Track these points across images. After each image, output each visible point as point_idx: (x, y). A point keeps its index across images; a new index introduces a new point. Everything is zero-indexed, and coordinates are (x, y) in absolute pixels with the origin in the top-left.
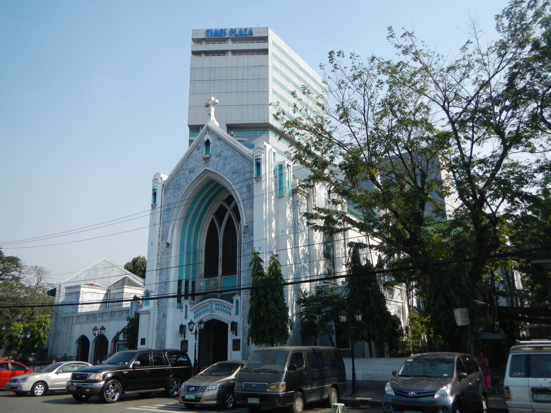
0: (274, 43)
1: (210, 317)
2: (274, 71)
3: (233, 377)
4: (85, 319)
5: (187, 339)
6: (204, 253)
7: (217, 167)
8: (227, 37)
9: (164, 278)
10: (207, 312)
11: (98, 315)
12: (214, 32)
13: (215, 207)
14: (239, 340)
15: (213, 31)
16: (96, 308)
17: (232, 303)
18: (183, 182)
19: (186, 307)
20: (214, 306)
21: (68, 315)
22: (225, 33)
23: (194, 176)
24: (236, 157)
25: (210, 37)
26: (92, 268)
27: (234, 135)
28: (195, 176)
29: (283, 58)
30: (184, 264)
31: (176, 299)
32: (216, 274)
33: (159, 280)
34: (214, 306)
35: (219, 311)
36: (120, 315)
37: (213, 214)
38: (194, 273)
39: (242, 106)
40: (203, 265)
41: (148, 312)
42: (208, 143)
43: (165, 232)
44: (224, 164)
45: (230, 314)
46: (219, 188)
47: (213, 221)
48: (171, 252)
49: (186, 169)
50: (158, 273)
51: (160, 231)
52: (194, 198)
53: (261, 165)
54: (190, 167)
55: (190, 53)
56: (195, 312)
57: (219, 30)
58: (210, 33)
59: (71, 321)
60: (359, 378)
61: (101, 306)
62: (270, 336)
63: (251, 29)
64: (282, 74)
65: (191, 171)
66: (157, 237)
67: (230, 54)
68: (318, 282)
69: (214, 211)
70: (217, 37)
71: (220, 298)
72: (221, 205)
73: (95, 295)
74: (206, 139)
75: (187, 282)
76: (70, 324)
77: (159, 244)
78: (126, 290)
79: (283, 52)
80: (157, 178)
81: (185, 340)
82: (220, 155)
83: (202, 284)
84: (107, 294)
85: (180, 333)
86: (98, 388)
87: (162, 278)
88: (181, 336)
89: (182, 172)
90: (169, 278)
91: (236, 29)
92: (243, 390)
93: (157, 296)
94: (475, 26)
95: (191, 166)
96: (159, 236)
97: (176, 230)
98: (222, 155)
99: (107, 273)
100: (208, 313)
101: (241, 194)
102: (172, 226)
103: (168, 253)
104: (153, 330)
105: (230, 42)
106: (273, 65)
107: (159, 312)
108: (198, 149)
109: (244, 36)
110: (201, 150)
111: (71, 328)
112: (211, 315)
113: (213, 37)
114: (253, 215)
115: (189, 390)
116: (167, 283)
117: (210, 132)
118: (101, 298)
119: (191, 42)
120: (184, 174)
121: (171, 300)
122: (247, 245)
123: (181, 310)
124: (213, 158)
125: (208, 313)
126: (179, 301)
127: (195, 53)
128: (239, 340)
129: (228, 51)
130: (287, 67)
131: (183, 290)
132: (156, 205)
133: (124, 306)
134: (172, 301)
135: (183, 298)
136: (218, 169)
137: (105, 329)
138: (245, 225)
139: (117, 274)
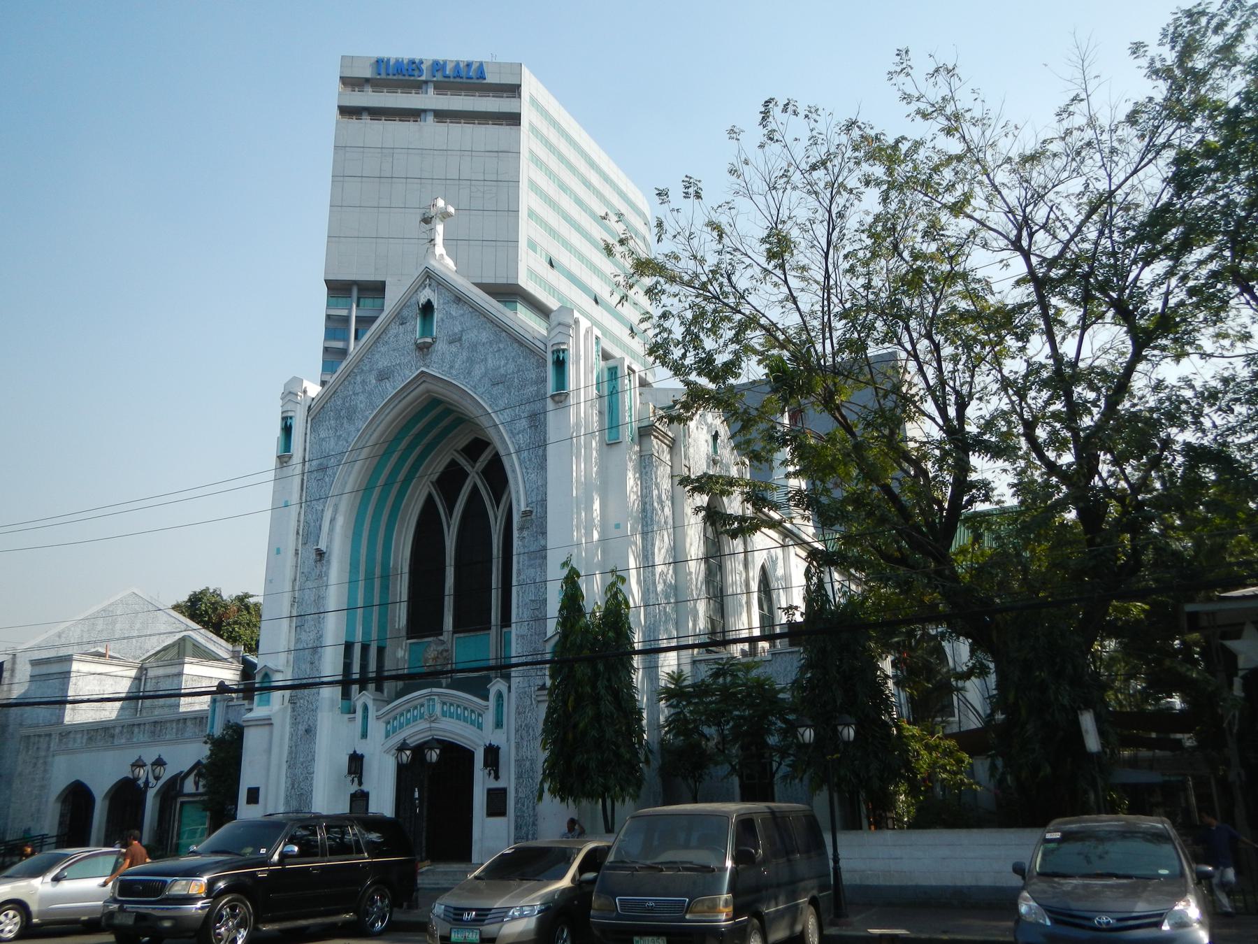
0: (534, 101)
1: (429, 733)
2: (532, 166)
3: (566, 882)
4: (84, 741)
5: (365, 788)
6: (406, 577)
7: (451, 367)
8: (423, 78)
9: (308, 638)
10: (419, 721)
11: (117, 730)
13: (437, 466)
14: (503, 791)
15: (392, 62)
16: (110, 712)
17: (486, 698)
18: (361, 401)
19: (366, 708)
20: (438, 708)
21: (38, 731)
22: (420, 70)
23: (391, 388)
24: (501, 346)
25: (383, 76)
26: (98, 612)
28: (394, 389)
29: (553, 137)
30: (360, 604)
31: (339, 689)
32: (437, 629)
33: (296, 643)
34: (438, 708)
35: (452, 720)
36: (177, 730)
37: (432, 483)
38: (382, 628)
39: (455, 242)
40: (404, 606)
41: (267, 722)
42: (427, 309)
43: (312, 524)
44: (470, 360)
45: (480, 727)
46: (451, 417)
47: (430, 497)
48: (327, 575)
49: (371, 370)
50: (294, 625)
51: (299, 521)
52: (387, 444)
53: (567, 365)
54: (380, 365)
55: (336, 111)
56: (388, 723)
57: (405, 62)
58: (383, 66)
59: (43, 746)
60: (846, 878)
61: (122, 708)
62: (601, 780)
63: (481, 64)
64: (550, 174)
65: (383, 376)
66: (292, 536)
68: (696, 651)
69: (435, 477)
70: (401, 77)
71: (448, 687)
72: (453, 463)
73: (110, 681)
74: (423, 300)
75: (365, 648)
76: (42, 753)
77: (297, 554)
78: (188, 669)
79: (554, 123)
80: (292, 390)
81: (362, 791)
82: (460, 339)
83: (400, 653)
84: (137, 679)
85: (350, 772)
86: (190, 918)
87: (304, 636)
88: (353, 781)
89: (358, 378)
90: (321, 636)
91: (445, 62)
92: (619, 917)
93: (289, 683)
94: (1086, 64)
95: (383, 363)
96: (298, 533)
97: (340, 521)
98: (464, 339)
99: (138, 626)
100: (423, 725)
101: (513, 434)
102: (331, 509)
103: (320, 576)
104: (280, 767)
105: (431, 91)
106: (531, 151)
107: (295, 722)
108: (402, 324)
109: (465, 80)
110: (409, 326)
111: (45, 763)
112: (430, 729)
113: (391, 77)
114: (545, 485)
115: (462, 920)
116: (316, 649)
117: (434, 283)
118: (123, 687)
119: (337, 85)
120: (364, 382)
121: (326, 692)
122: (530, 559)
123: (352, 716)
124: (441, 346)
125: (423, 725)
126: (346, 695)
127: (346, 111)
128: (503, 791)
129: (425, 111)
130: (562, 158)
131: (356, 668)
132: (290, 457)
133: (182, 709)
134: (329, 694)
135: (355, 688)
136: (454, 372)
137: (165, 764)
138: (523, 509)
139: (163, 628)
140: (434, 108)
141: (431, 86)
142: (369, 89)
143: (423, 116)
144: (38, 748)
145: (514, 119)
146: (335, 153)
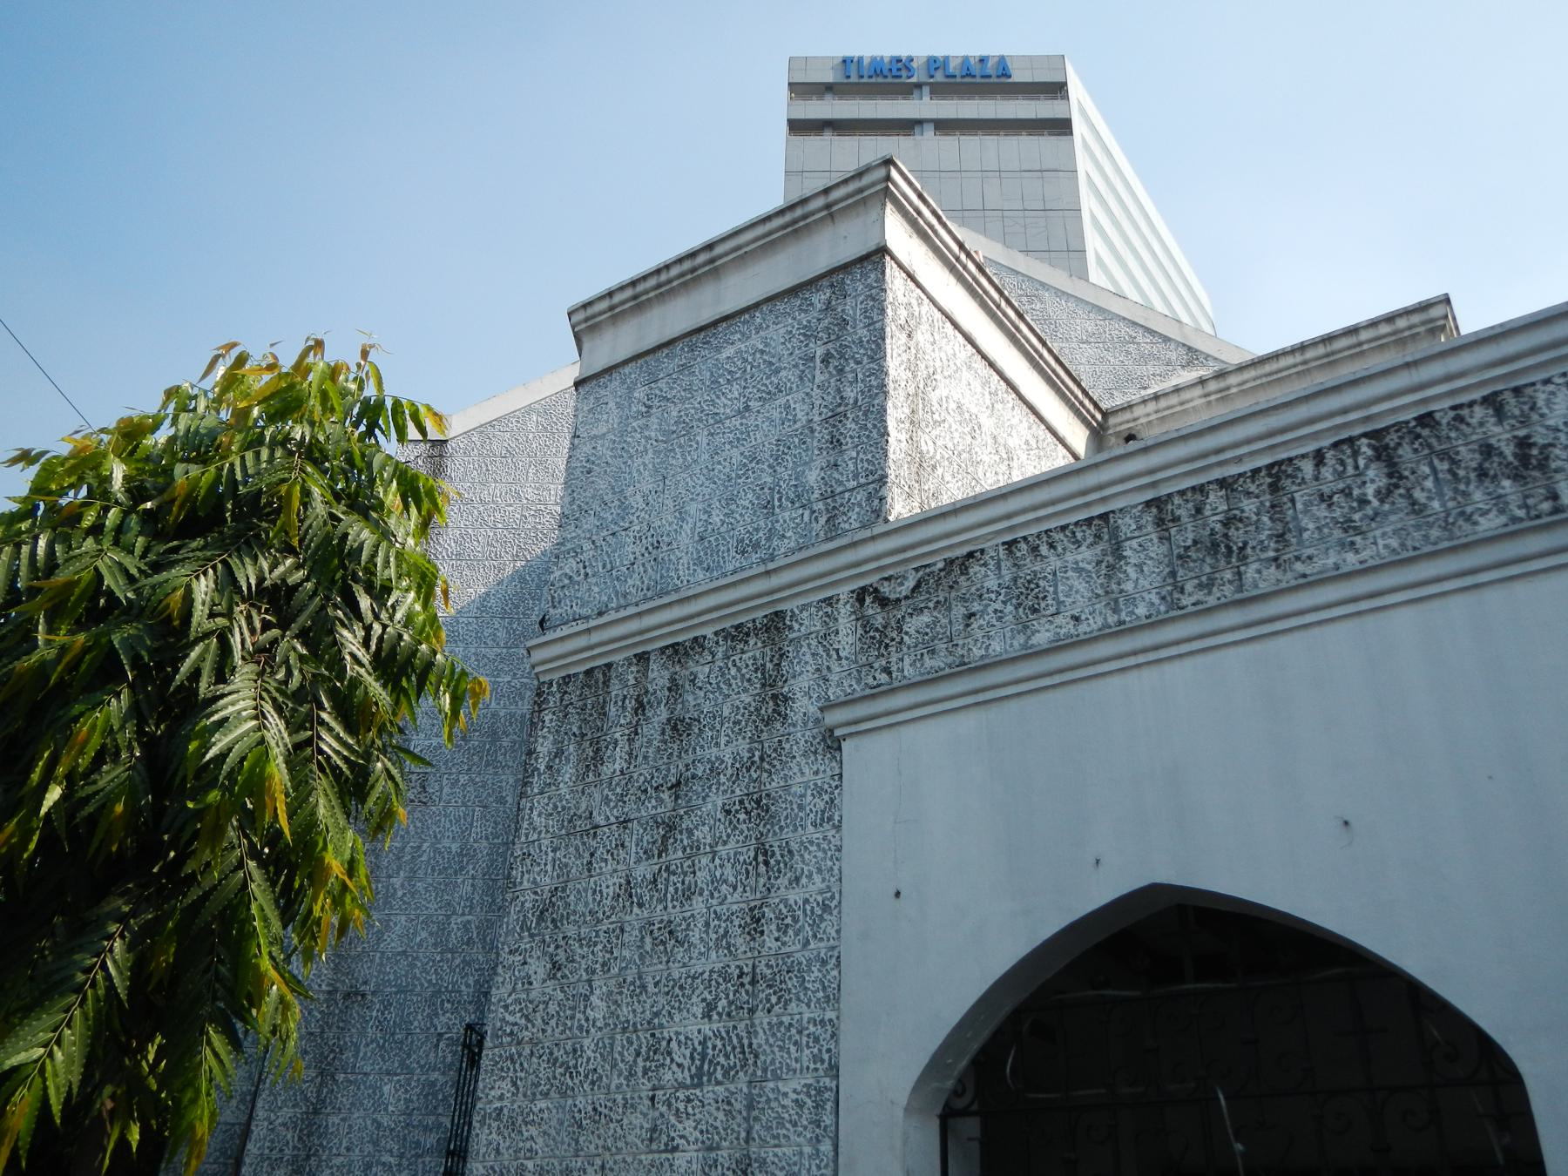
0: (1083, 111)
8: (914, 80)
12: (870, 64)
15: (866, 62)
21: (664, 622)
22: (908, 69)
25: (854, 79)
57: (886, 60)
63: (1002, 58)
67: (929, 131)
70: (880, 80)
91: (946, 58)
105: (926, 99)
109: (978, 80)
113: (865, 80)
129: (920, 122)
140: (934, 116)
141: (926, 90)
142: (828, 97)
143: (917, 129)
144: (678, 727)
145: (1062, 127)
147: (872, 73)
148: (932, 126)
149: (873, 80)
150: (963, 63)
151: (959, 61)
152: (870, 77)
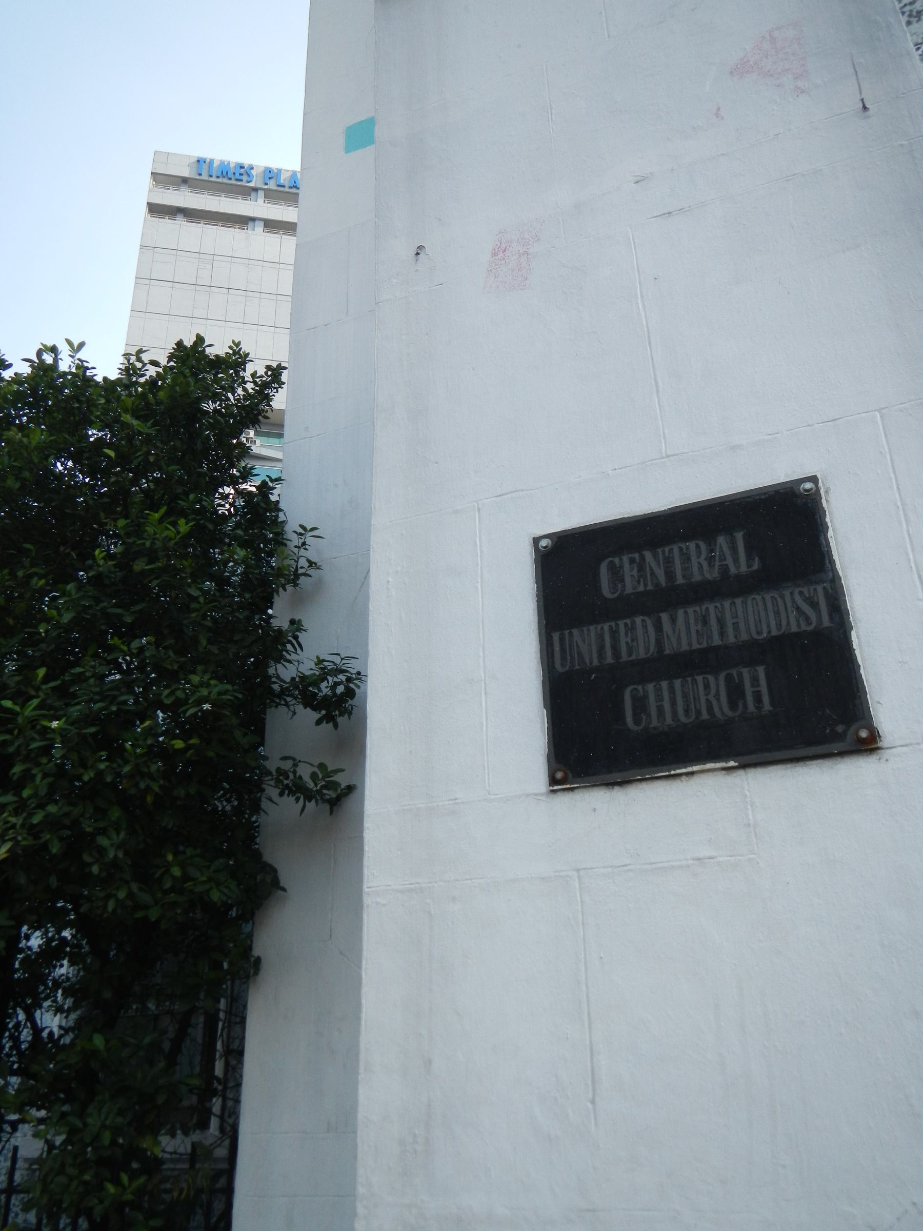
8: (252, 184)
12: (219, 166)
22: (249, 175)
25: (205, 177)
27: (258, 442)
55: (144, 208)
57: (232, 165)
58: (205, 167)
67: (259, 227)
70: (226, 181)
91: (280, 170)
105: (261, 200)
113: (213, 179)
119: (147, 180)
127: (155, 209)
129: (253, 219)
140: (264, 216)
141: (261, 194)
143: (251, 224)
146: (141, 253)
147: (220, 174)
148: (262, 223)
149: (220, 180)
150: (291, 176)
151: (288, 174)
152: (218, 177)
